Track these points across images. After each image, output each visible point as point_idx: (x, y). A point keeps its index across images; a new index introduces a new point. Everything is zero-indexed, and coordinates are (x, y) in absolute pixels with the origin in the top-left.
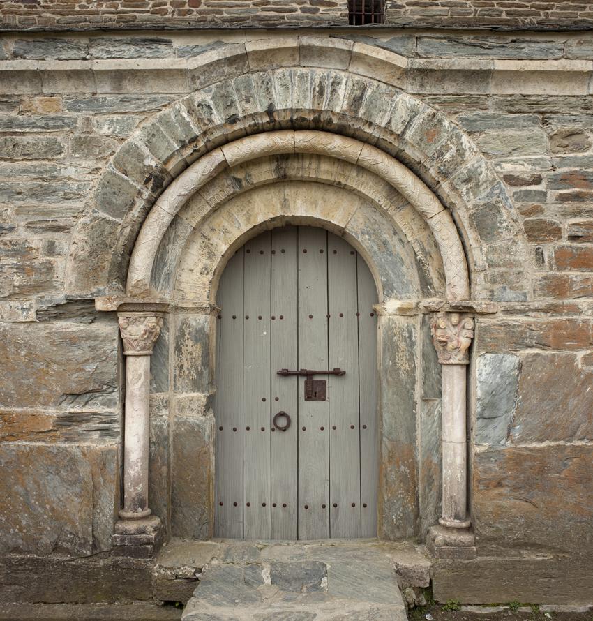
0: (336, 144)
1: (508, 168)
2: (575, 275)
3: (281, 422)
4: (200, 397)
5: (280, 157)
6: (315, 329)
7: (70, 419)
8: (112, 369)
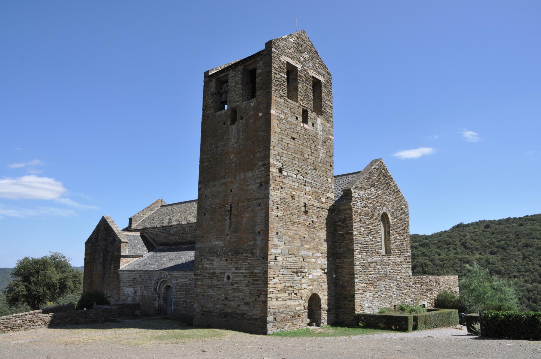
7: (153, 303)
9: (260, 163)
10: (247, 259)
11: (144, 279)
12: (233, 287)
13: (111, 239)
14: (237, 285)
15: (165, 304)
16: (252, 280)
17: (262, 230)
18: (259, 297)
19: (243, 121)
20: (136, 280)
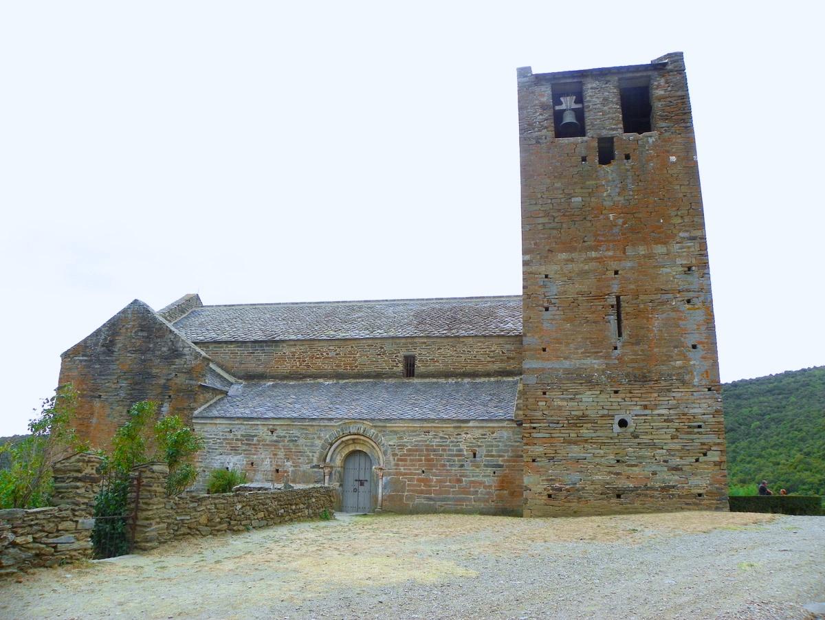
0: (362, 438)
1: (390, 443)
2: (400, 463)
3: (355, 490)
4: (338, 484)
5: (353, 439)
6: (362, 472)
8: (322, 478)
9: (682, 234)
10: (669, 390)
11: (285, 437)
12: (637, 440)
13: (164, 349)
14: (650, 437)
15: (341, 489)
16: (686, 427)
17: (701, 343)
18: (705, 455)
19: (628, 164)
20: (255, 439)
